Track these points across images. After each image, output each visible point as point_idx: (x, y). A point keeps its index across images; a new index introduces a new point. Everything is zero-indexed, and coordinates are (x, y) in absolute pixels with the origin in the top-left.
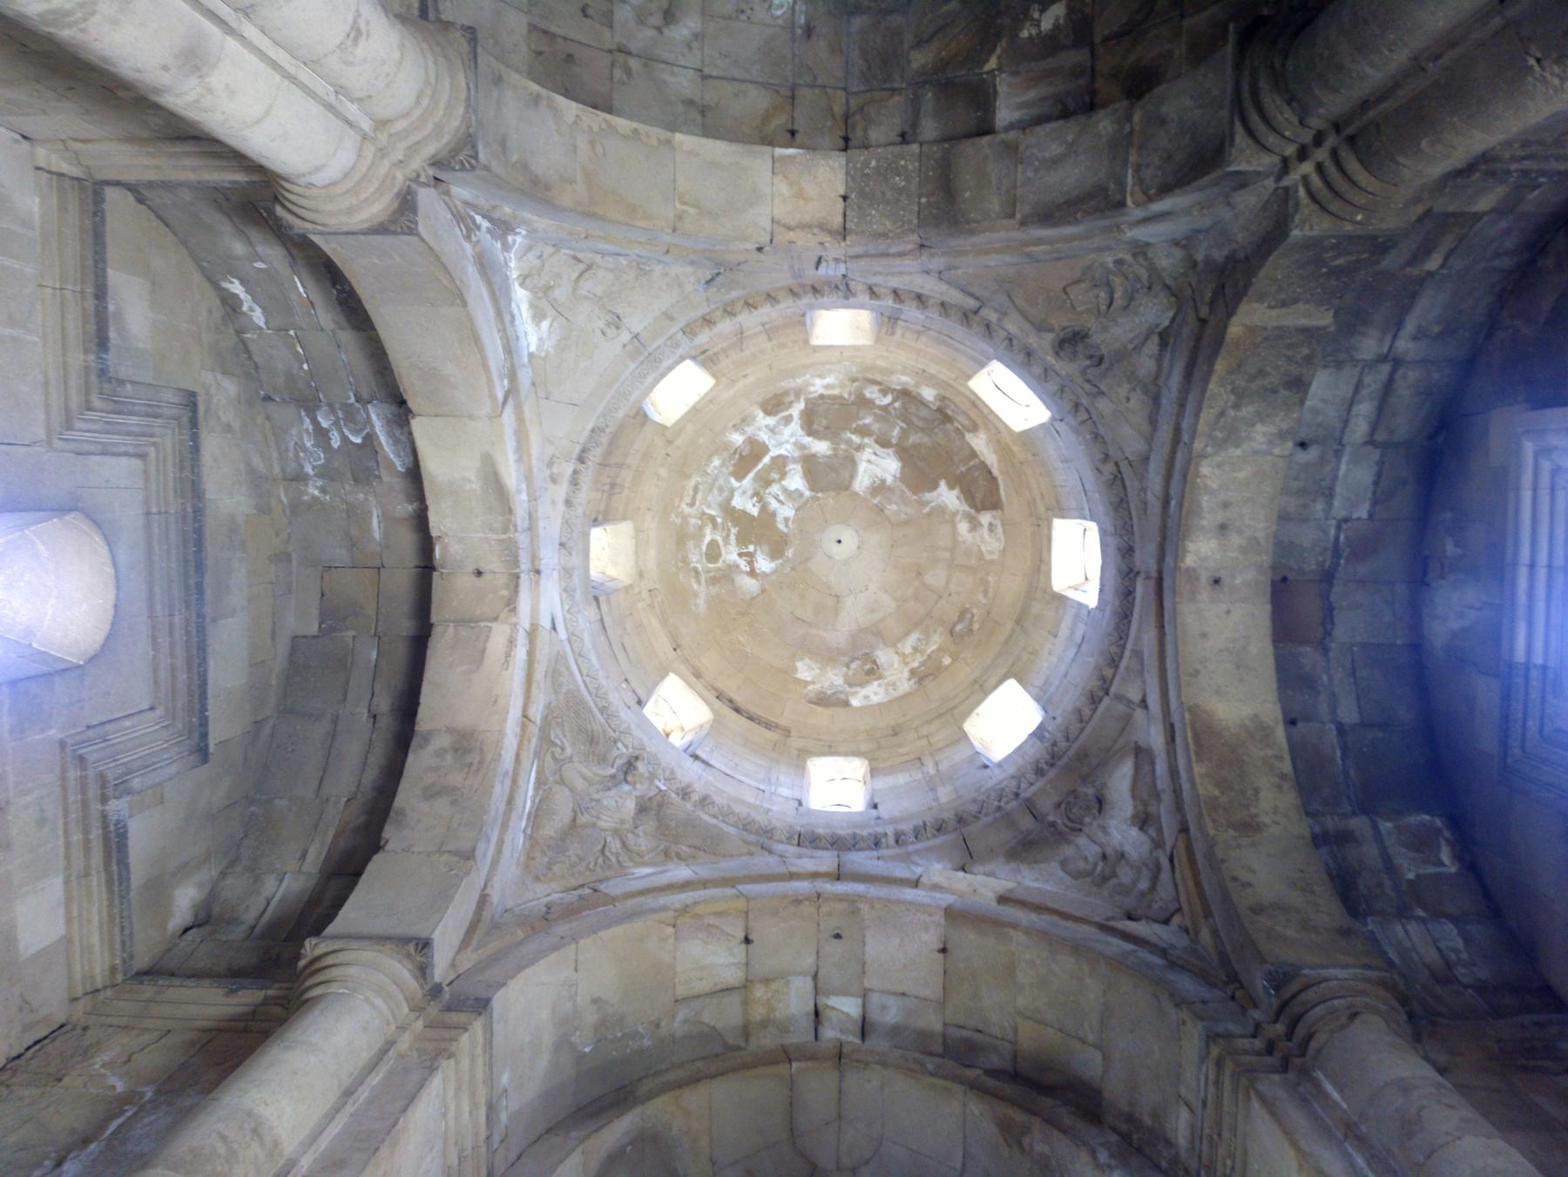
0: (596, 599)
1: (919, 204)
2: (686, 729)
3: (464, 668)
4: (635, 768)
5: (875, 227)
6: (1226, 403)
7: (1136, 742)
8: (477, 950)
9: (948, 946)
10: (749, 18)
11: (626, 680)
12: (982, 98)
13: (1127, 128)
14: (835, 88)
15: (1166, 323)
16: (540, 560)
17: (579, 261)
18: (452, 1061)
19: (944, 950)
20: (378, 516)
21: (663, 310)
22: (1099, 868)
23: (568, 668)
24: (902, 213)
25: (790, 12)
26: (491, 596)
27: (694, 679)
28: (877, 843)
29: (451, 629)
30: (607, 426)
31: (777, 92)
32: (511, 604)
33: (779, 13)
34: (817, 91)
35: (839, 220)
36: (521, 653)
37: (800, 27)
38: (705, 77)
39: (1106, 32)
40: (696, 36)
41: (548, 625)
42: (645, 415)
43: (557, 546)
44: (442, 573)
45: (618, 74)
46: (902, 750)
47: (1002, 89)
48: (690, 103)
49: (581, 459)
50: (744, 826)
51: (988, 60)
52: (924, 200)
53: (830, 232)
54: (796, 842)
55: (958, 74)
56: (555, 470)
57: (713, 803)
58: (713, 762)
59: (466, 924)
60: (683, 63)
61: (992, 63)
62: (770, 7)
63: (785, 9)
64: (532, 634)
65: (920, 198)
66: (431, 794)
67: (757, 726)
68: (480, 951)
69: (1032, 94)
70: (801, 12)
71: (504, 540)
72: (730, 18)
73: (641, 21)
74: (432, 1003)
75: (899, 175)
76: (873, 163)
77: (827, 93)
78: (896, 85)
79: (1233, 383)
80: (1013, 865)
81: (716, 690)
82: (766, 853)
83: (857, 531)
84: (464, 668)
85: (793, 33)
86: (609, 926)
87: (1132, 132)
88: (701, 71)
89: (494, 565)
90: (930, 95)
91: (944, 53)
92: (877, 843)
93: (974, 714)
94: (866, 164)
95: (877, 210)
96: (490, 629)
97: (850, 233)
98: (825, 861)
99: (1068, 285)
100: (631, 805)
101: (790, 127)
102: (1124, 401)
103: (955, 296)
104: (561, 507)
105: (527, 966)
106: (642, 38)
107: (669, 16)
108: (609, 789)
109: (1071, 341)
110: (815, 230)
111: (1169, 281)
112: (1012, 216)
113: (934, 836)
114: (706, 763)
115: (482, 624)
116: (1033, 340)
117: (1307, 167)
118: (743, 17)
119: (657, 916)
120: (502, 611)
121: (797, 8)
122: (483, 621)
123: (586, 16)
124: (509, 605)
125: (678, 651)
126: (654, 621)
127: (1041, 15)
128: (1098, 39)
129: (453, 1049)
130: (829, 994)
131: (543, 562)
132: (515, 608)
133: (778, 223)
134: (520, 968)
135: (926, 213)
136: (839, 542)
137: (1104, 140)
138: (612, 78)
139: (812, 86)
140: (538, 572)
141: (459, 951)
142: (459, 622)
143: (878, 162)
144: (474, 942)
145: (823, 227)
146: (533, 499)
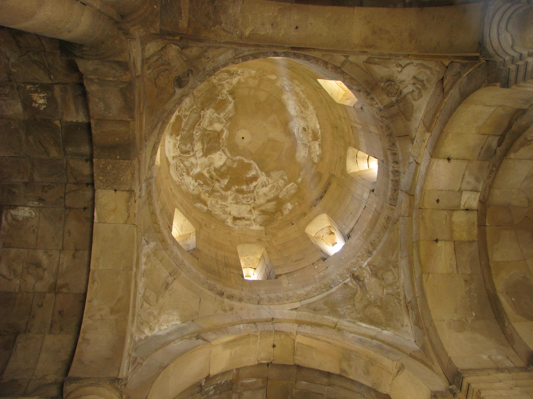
0: (277, 277)
1: (119, 159)
2: (330, 225)
3: (314, 354)
4: (358, 276)
5: (129, 178)
6: (219, 28)
7: (363, 62)
8: (433, 363)
9: (447, 157)
10: (36, 228)
11: (313, 264)
12: (72, 128)
13: (97, 80)
14: (65, 188)
15: (178, 47)
16: (268, 318)
17: (142, 305)
18: (481, 392)
19: (449, 159)
20: (247, 380)
21: (159, 262)
22: (419, 87)
23: (313, 302)
24: (123, 167)
25: (33, 209)
26: (284, 342)
27: (306, 217)
28: (396, 173)
29: (297, 358)
30: (207, 283)
31: (67, 215)
32: (287, 334)
33: (34, 214)
34: (67, 197)
35: (125, 193)
36: (308, 330)
37: (39, 204)
38: (63, 249)
39: (47, 78)
40: (46, 252)
41: (295, 312)
42: (194, 249)
43: (260, 306)
44: (273, 360)
45: (65, 290)
46: (346, 130)
47: (69, 119)
48: (74, 256)
49: (222, 294)
50: (385, 228)
51: (56, 126)
52: (118, 157)
53: (131, 197)
54: (394, 207)
55: (61, 137)
56: (227, 308)
57: (374, 241)
58: (351, 227)
59: (422, 366)
60: (58, 259)
61: (57, 122)
62: (31, 218)
63: (32, 211)
64: (300, 323)
65: (117, 159)
66: (367, 372)
67: (329, 189)
68: (434, 362)
69: (72, 107)
70: (33, 203)
71: (261, 337)
72: (37, 236)
73: (41, 279)
74: (457, 395)
75: (106, 167)
76: (101, 178)
77: (68, 193)
78: (65, 162)
79: (211, 27)
80: (413, 120)
81: (311, 207)
82: (398, 222)
83: (239, 130)
84: (314, 354)
85: (42, 207)
86: (427, 304)
87: (98, 79)
88: (60, 251)
89: (270, 341)
90: (70, 149)
91: (52, 143)
92: (396, 173)
93: (332, 96)
94: (101, 181)
95: (122, 177)
96: (297, 342)
97: (131, 189)
98: (402, 197)
99: (156, 87)
100: (374, 280)
101: (83, 210)
102: (209, 59)
103: (156, 132)
104: (243, 304)
105: (443, 345)
106: (49, 278)
107: (38, 265)
108: (366, 289)
109: (180, 82)
110: (130, 204)
111: (159, 48)
112: (129, 122)
113: (396, 147)
114: (352, 230)
115: (296, 345)
116: (176, 97)
117: (132, 30)
118: (36, 230)
119: (424, 281)
120: (291, 338)
121: (31, 205)
122: (294, 345)
123: (42, 305)
124: (288, 335)
125: (294, 223)
126: (280, 234)
127: (37, 103)
128: (50, 82)
129: (476, 390)
130: (460, 205)
131: (269, 317)
132: (289, 333)
133: (127, 221)
134: (443, 348)
135: (124, 156)
136: (243, 138)
137: (100, 88)
138: (67, 293)
139: (65, 199)
140: (273, 319)
141: (433, 371)
142: (294, 354)
143: (100, 176)
144: (430, 363)
145: (128, 201)
146: (242, 322)
